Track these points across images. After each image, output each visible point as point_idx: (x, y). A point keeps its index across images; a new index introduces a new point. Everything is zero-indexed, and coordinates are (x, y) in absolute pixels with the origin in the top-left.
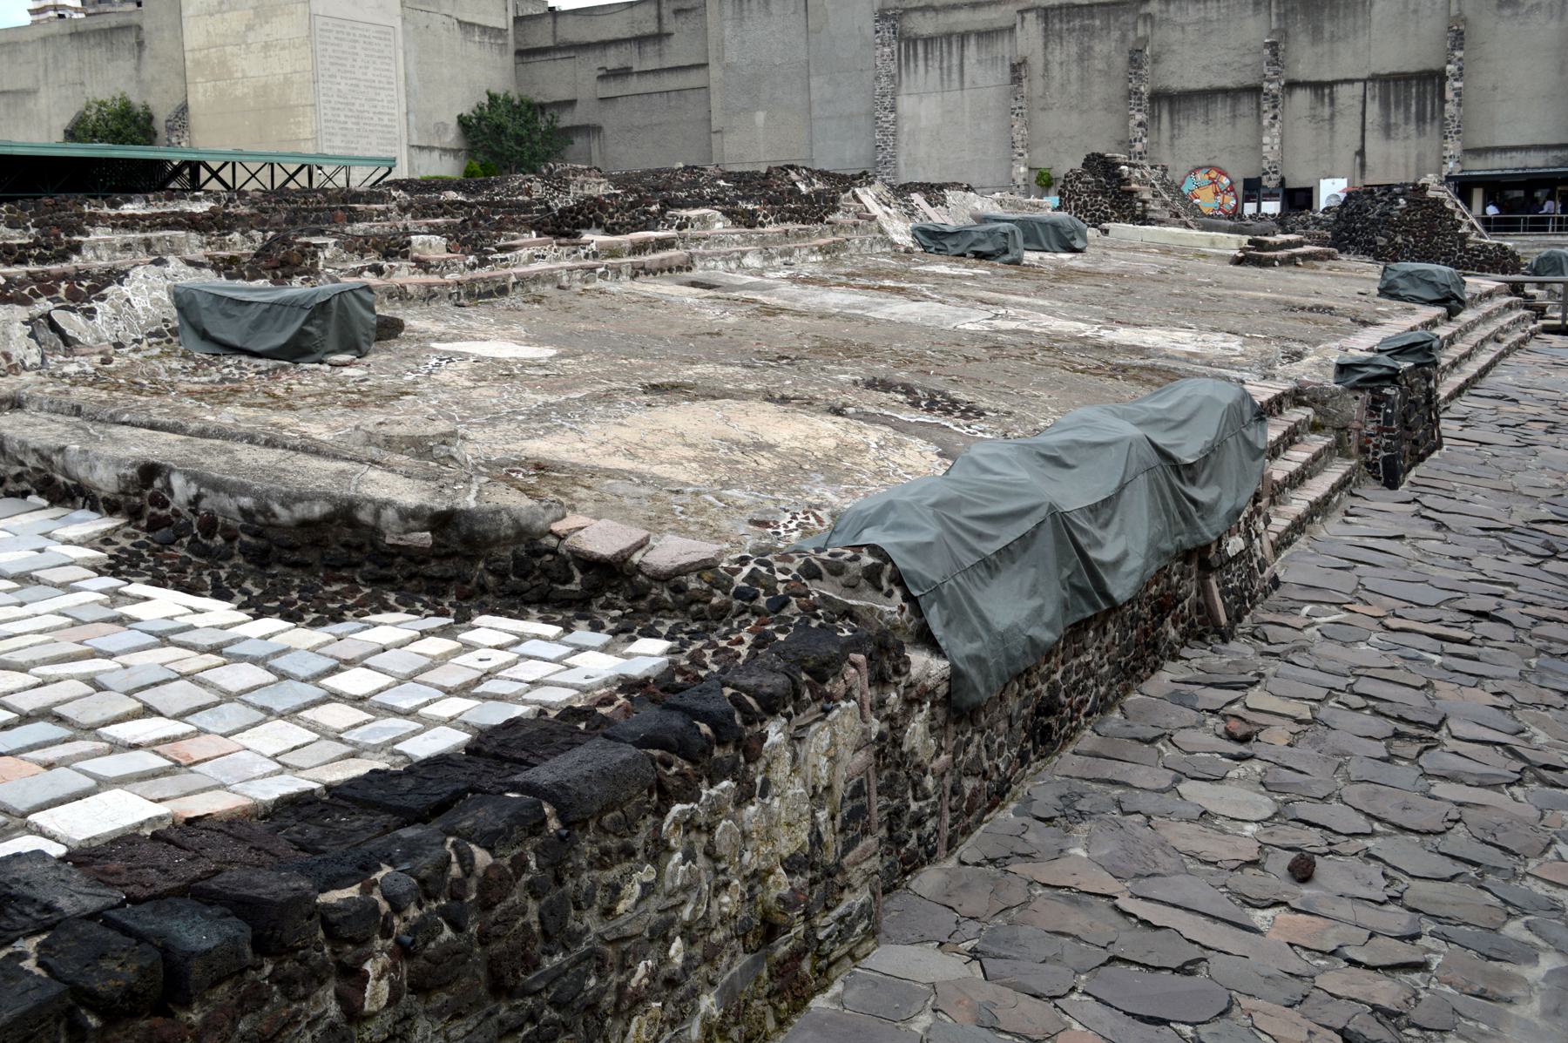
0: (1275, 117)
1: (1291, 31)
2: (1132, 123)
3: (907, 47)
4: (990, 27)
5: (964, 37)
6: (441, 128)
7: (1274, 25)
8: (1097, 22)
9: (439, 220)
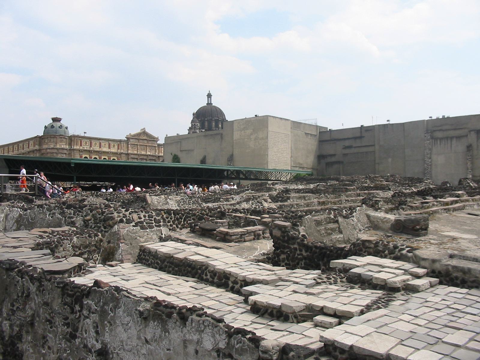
5: (452, 138)
9: (365, 192)
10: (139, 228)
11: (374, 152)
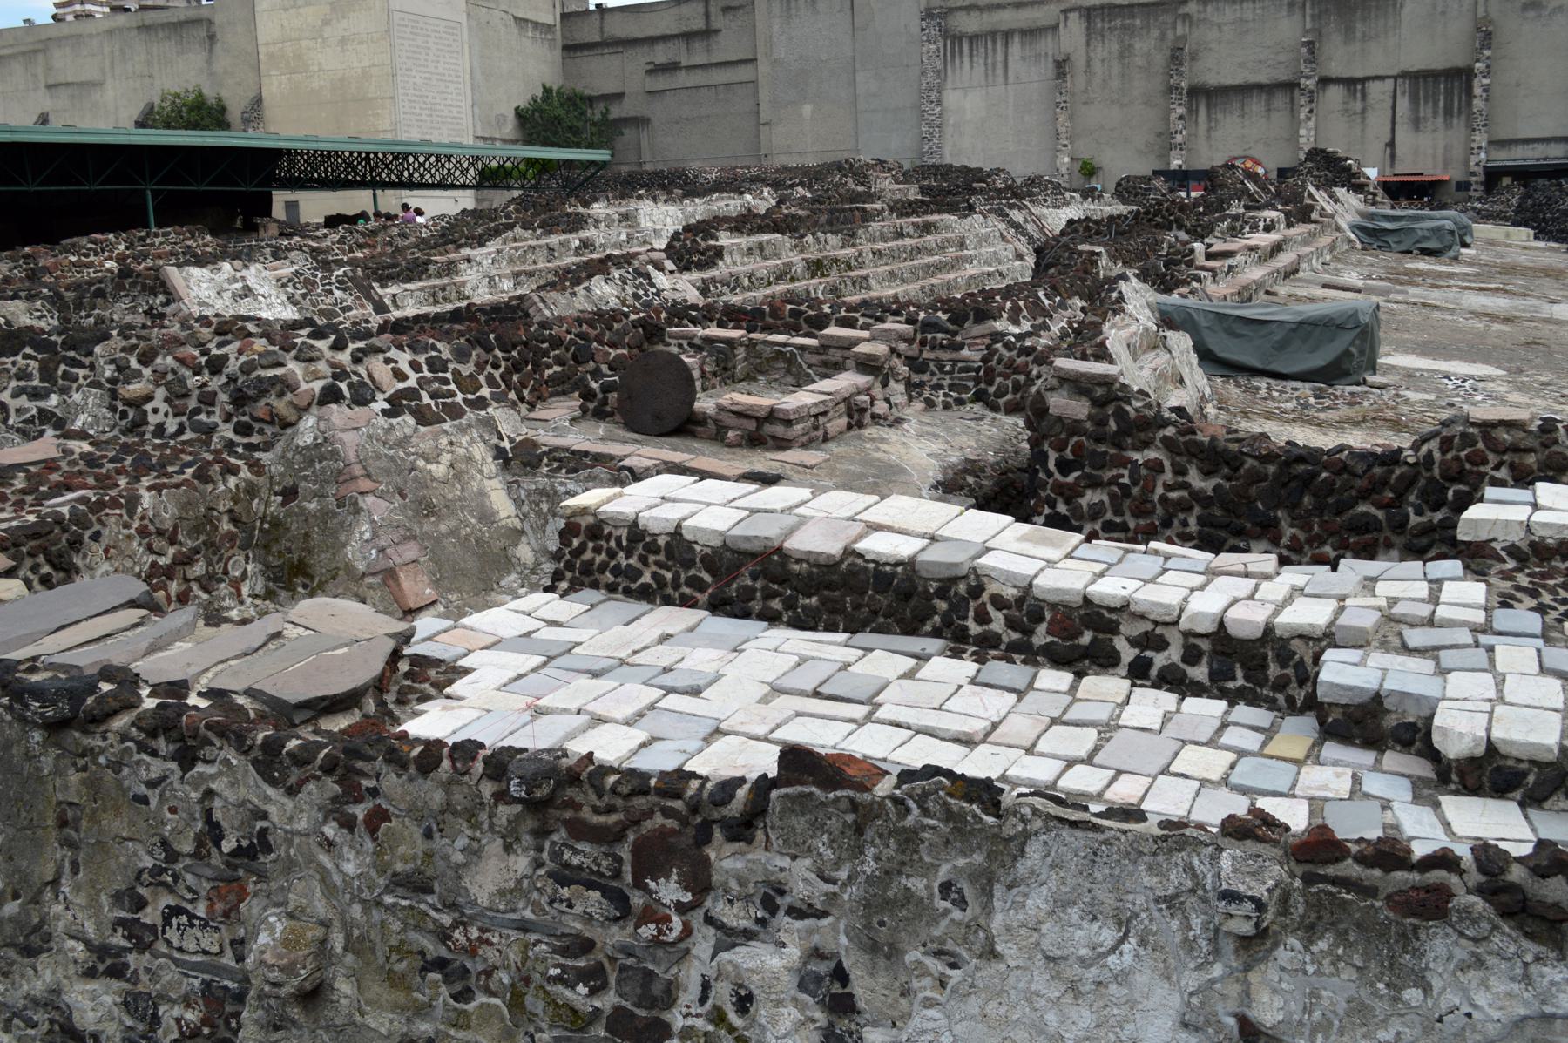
0: (1311, 111)
1: (1324, 31)
2: (1173, 116)
3: (953, 44)
4: (1033, 26)
5: (1008, 35)
6: (501, 119)
7: (1309, 25)
8: (1138, 22)
10: (410, 420)
11: (754, 82)
